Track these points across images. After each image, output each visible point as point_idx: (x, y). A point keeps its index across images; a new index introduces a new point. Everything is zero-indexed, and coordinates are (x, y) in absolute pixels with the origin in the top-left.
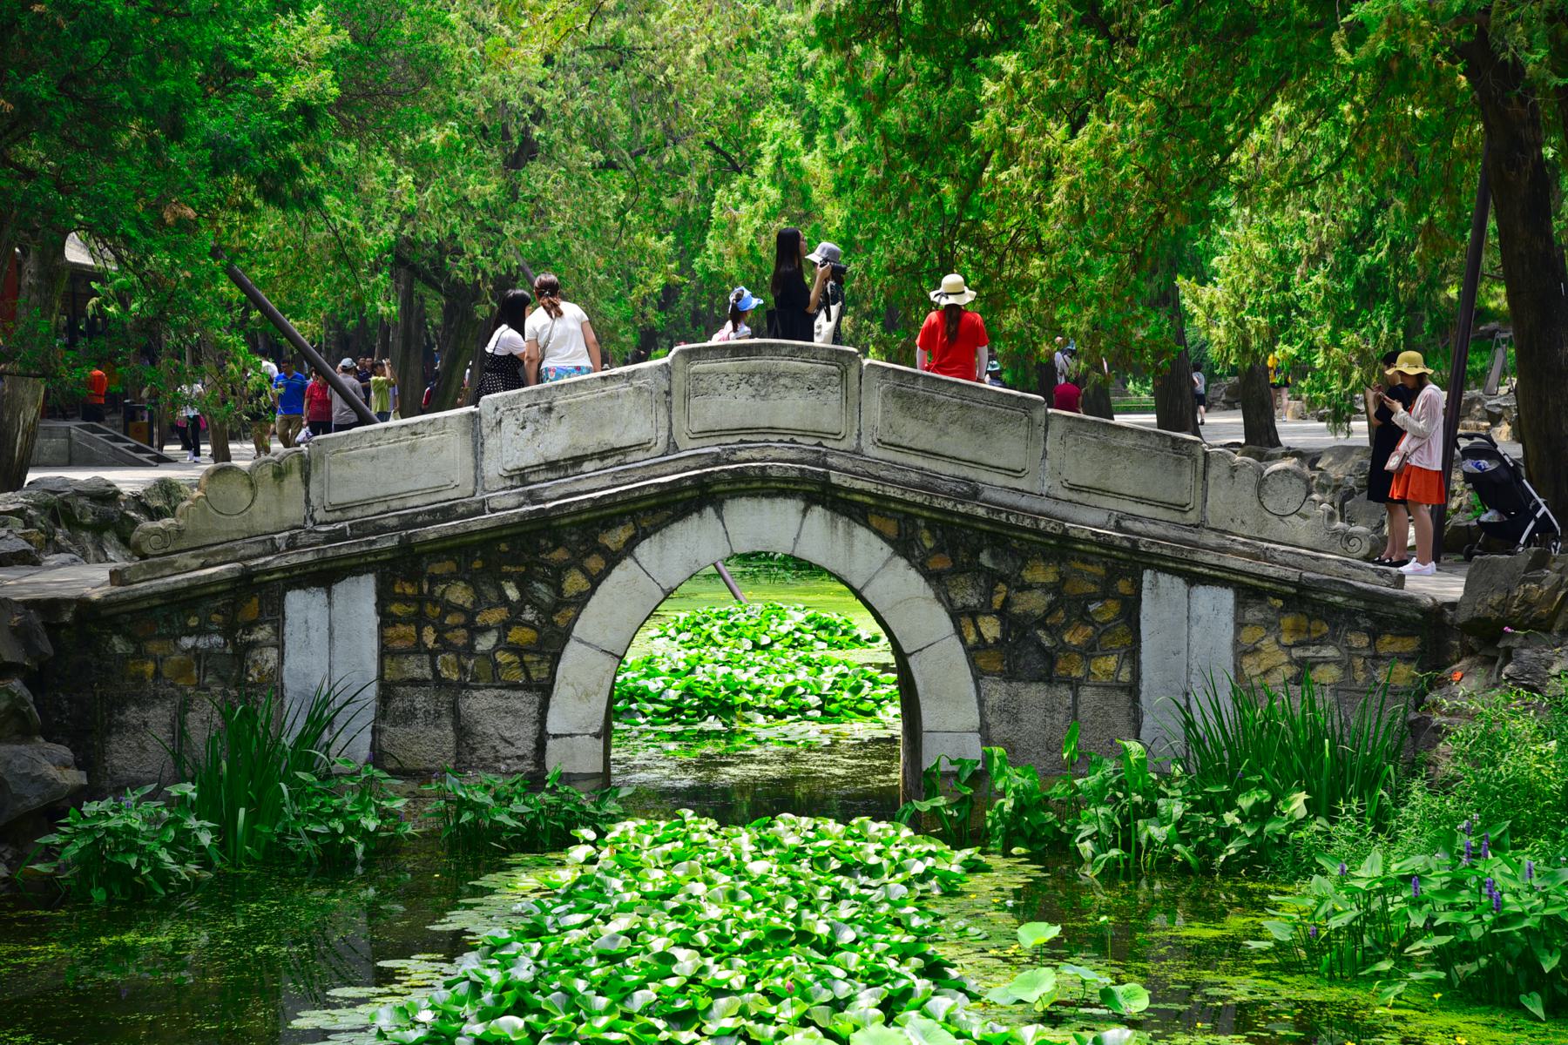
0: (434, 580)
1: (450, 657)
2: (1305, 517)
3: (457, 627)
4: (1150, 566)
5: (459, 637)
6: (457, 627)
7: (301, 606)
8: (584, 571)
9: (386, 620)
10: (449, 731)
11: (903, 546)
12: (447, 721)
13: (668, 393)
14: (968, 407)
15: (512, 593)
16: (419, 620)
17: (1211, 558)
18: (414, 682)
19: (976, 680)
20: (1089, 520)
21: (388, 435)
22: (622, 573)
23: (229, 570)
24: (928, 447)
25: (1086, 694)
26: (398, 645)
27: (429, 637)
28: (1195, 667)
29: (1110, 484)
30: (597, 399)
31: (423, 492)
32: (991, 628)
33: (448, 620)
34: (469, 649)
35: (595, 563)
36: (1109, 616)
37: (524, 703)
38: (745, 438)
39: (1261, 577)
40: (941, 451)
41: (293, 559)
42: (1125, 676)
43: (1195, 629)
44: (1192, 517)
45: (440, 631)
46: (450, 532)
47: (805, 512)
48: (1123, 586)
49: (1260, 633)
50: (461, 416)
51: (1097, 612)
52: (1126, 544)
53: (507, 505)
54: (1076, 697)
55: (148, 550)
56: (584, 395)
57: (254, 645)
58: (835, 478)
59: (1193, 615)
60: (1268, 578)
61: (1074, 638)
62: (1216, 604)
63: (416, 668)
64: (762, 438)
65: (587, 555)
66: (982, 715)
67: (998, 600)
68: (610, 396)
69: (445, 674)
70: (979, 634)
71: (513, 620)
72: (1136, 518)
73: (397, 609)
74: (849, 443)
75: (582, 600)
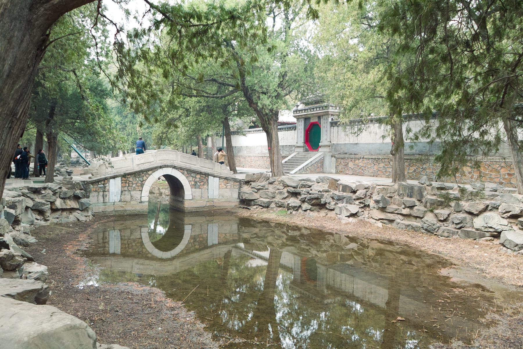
5: (131, 185)
7: (111, 180)
9: (122, 183)
11: (183, 173)
16: (126, 183)
20: (204, 170)
27: (127, 185)
32: (193, 183)
34: (132, 187)
37: (139, 192)
45: (129, 184)
53: (137, 169)
63: (126, 189)
75: (145, 180)
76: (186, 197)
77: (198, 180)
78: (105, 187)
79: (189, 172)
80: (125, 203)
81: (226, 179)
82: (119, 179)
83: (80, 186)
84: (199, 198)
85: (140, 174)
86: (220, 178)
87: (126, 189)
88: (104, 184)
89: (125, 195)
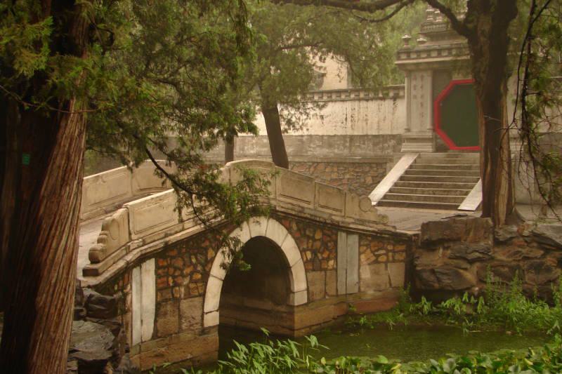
10: (177, 317)
15: (194, 260)
33: (176, 274)
43: (349, 249)
58: (277, 209)
86: (362, 235)
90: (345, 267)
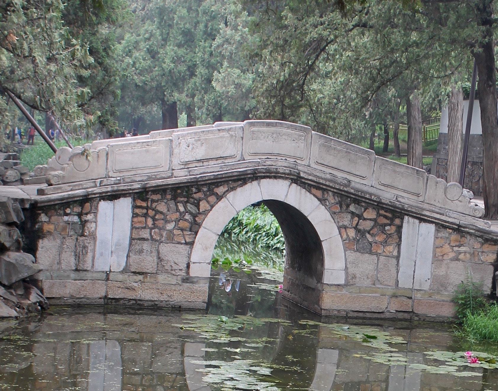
0: (153, 201)
1: (157, 230)
2: (461, 202)
3: (160, 219)
4: (408, 215)
5: (160, 223)
6: (160, 219)
7: (104, 205)
8: (208, 202)
9: (135, 215)
10: (155, 258)
11: (322, 201)
12: (155, 254)
13: (242, 138)
14: (349, 152)
15: (182, 209)
16: (146, 215)
17: (428, 213)
18: (144, 239)
19: (345, 251)
20: (387, 196)
21: (138, 145)
22: (221, 204)
23: (81, 192)
24: (333, 166)
25: (382, 258)
26: (138, 225)
27: (150, 222)
28: (419, 251)
29: (393, 184)
30: (216, 138)
31: (150, 168)
32: (352, 233)
33: (157, 217)
35: (212, 199)
36: (392, 231)
37: (183, 249)
38: (269, 157)
39: (445, 222)
40: (338, 168)
41: (104, 189)
42: (395, 253)
43: (420, 238)
44: (421, 199)
45: (154, 219)
46: (161, 184)
47: (259, 184)
48: (397, 221)
49: (443, 242)
50: (166, 140)
51: (388, 230)
52: (400, 206)
53: (181, 176)
54: (378, 260)
55: (52, 182)
56: (211, 136)
57: (86, 221)
58: (302, 175)
59: (420, 233)
60: (448, 222)
61: (378, 239)
62: (430, 229)
63: (145, 234)
64: (275, 157)
65: (210, 195)
66: (346, 264)
67: (355, 223)
68: (221, 137)
69: (155, 237)
70: (348, 235)
71: (182, 217)
72: (403, 197)
73: (137, 211)
74: (305, 162)
75: (206, 213)
76: (327, 279)
77: (366, 225)
78: (84, 223)
79: (346, 199)
80: (141, 277)
81: (459, 229)
82: (125, 205)
83: (7, 213)
84: (367, 283)
85: (193, 193)
86: (441, 226)
87: (145, 234)
88: (80, 215)
89: (141, 251)
90: (414, 258)
